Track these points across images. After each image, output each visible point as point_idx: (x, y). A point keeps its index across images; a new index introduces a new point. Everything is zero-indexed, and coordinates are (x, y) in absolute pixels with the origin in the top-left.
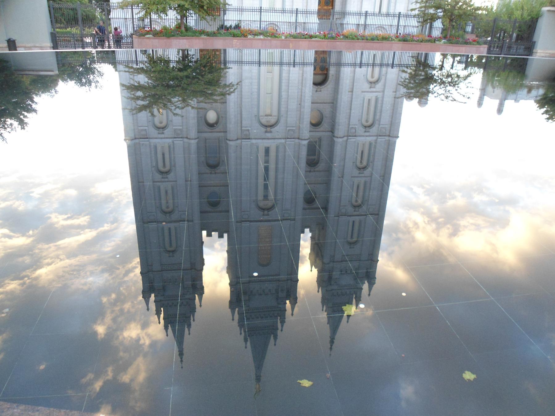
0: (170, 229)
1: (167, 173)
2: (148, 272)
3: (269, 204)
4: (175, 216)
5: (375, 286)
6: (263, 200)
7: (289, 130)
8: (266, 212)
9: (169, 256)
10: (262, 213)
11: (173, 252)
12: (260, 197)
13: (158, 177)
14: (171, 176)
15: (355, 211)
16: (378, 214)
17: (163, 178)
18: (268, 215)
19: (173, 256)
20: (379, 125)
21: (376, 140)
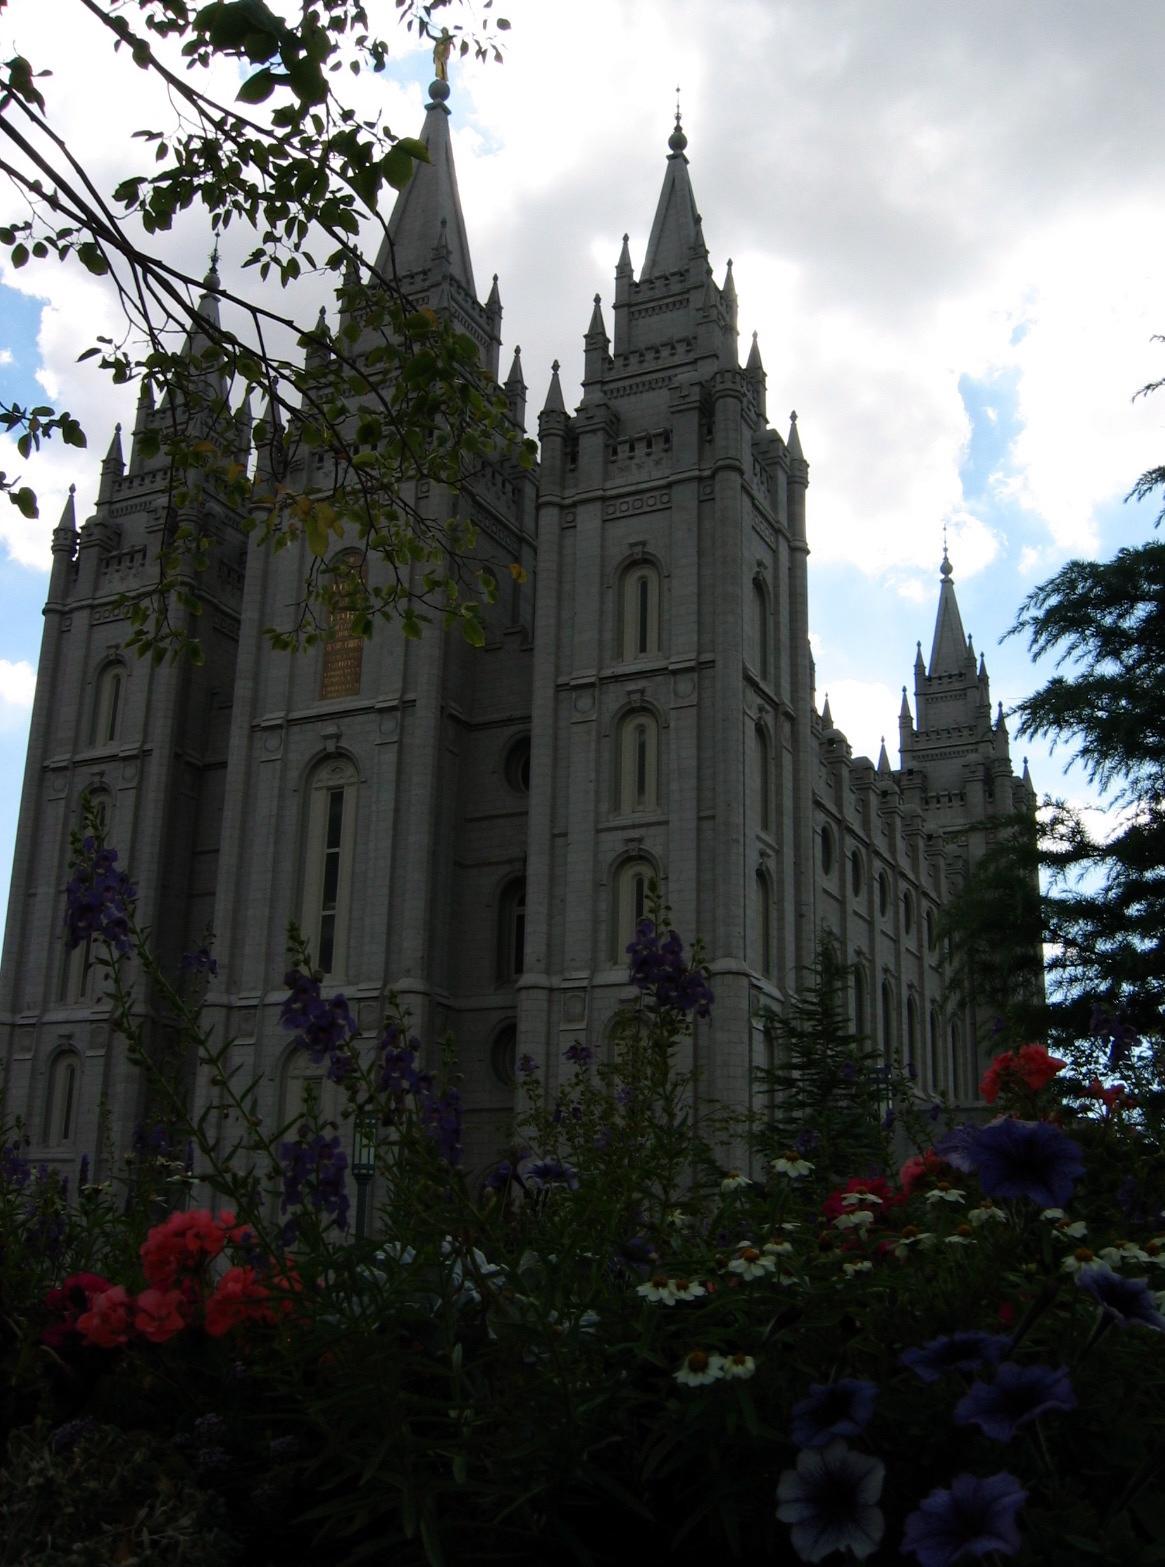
0: (643, 649)
1: (626, 860)
2: (712, 477)
3: (325, 777)
4: (614, 699)
5: (56, 525)
6: (341, 787)
7: (251, 1035)
8: (331, 747)
9: (643, 544)
10: (343, 744)
11: (631, 564)
12: (349, 795)
13: (654, 845)
14: (613, 845)
15: (102, 774)
16: (45, 769)
17: (640, 840)
18: (326, 737)
19: (632, 545)
20: (34, 1059)
21: (45, 1010)
